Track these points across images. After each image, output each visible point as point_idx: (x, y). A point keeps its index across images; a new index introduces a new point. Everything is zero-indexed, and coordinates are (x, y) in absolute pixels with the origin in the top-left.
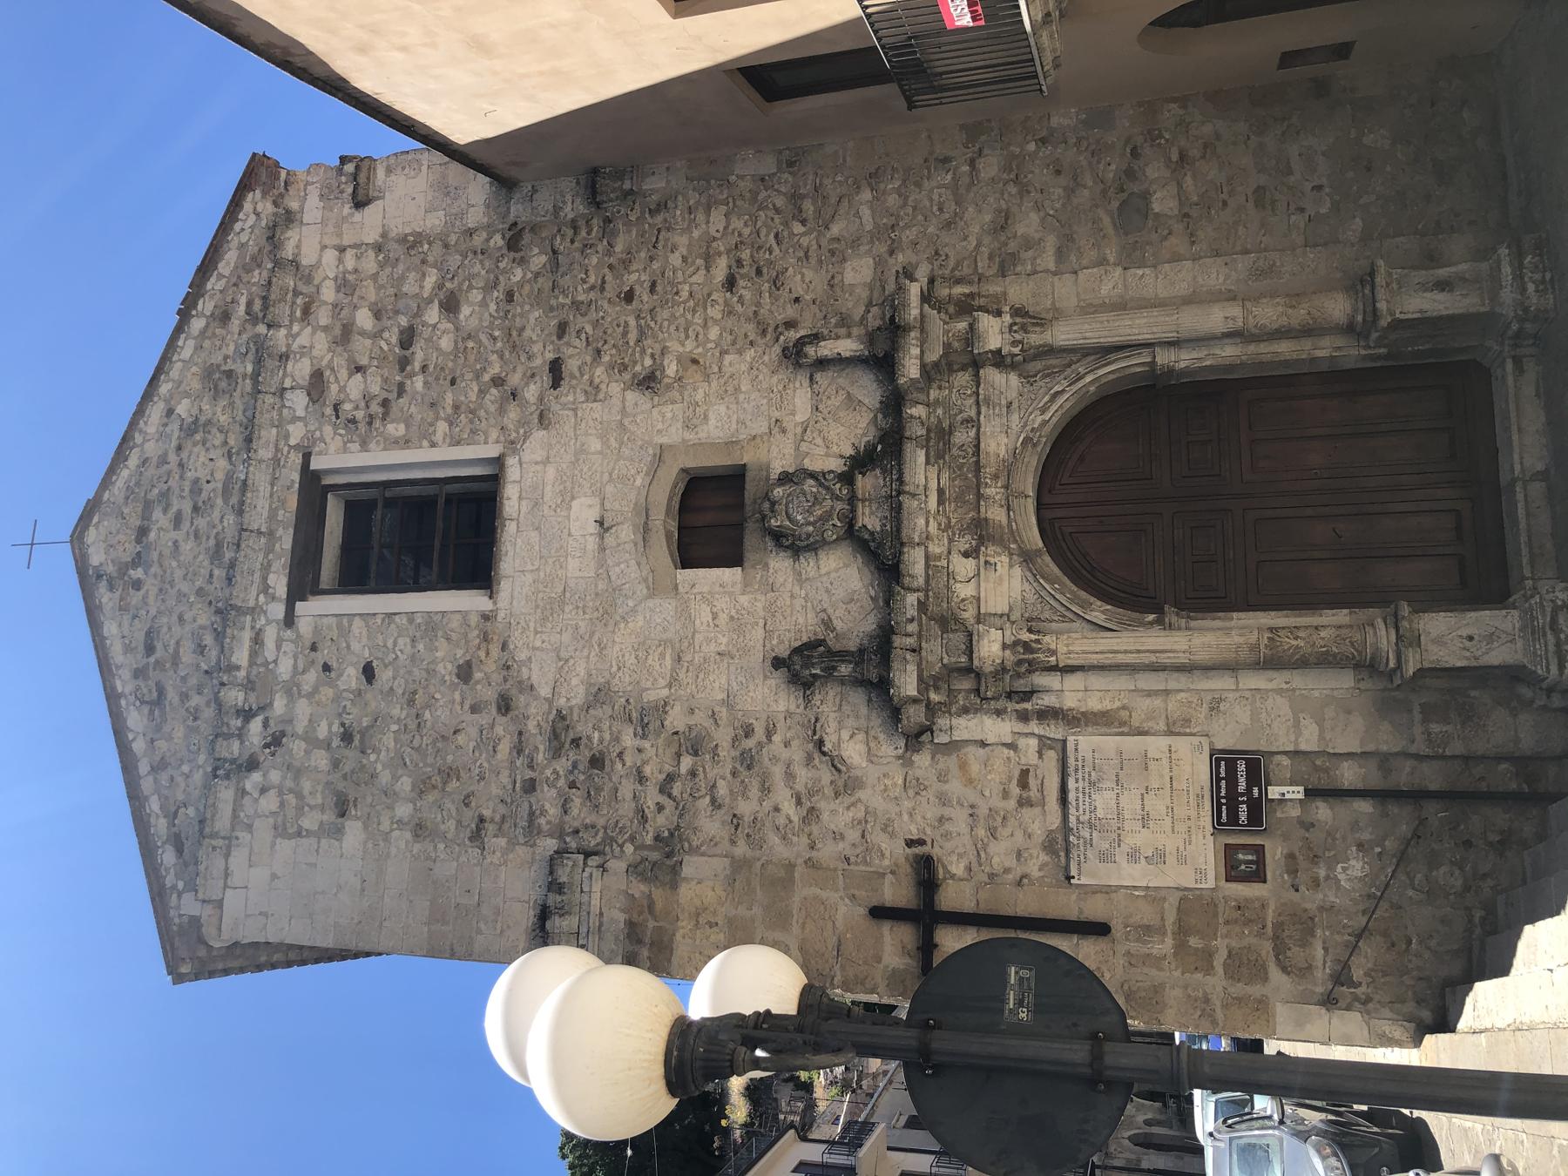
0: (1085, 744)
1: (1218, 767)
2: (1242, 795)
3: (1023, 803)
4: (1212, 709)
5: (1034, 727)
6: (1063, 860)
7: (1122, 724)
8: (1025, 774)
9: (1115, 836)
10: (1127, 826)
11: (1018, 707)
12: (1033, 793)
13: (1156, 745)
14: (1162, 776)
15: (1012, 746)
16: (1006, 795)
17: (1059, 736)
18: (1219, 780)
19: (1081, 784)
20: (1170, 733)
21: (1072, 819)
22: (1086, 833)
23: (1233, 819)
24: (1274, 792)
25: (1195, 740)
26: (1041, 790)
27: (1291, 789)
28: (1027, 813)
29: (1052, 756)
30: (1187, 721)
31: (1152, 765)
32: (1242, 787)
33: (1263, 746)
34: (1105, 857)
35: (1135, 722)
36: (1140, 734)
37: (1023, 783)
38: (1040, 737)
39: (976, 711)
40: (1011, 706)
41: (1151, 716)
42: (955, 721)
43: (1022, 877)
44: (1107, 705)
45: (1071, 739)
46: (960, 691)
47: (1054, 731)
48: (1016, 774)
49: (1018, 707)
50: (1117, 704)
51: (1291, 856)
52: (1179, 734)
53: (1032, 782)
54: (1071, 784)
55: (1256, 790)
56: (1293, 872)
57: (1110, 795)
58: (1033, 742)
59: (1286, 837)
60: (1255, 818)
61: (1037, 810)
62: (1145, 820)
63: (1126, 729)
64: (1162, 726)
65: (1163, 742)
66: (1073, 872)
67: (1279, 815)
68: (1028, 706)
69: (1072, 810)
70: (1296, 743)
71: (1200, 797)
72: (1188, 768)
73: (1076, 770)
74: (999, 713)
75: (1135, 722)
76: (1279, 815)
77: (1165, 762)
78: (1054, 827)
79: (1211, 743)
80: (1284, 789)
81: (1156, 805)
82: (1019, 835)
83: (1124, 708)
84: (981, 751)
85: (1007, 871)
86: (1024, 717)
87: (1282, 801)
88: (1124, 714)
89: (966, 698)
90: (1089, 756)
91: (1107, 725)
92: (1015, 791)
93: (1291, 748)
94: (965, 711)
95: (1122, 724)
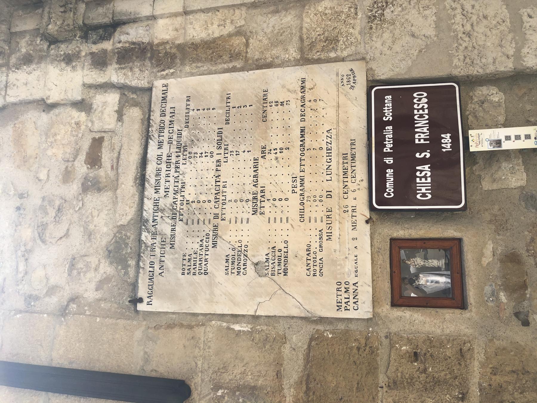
0: (178, 87)
1: (380, 104)
2: (422, 148)
3: (91, 186)
4: (371, 19)
5: (113, 74)
6: (132, 272)
7: (234, 56)
8: (97, 143)
9: (208, 229)
10: (230, 211)
11: (95, 48)
12: (105, 172)
13: (282, 81)
14: (287, 129)
15: (83, 105)
16: (67, 176)
17: (144, 83)
18: (381, 125)
19: (165, 150)
20: (304, 60)
21: (148, 205)
22: (165, 228)
23: (406, 189)
24: (481, 140)
25: (343, 68)
26: (116, 167)
27: (512, 131)
28: (94, 201)
29: (134, 114)
30: (332, 41)
31: (274, 113)
32: (422, 134)
33: (459, 68)
34: (193, 265)
35: (254, 53)
36: (260, 67)
37: (94, 160)
38: (122, 88)
39: (41, 59)
40: (86, 48)
41: (277, 40)
42: (12, 76)
43: (72, 300)
44: (215, 31)
45: (159, 84)
46: (22, 34)
47: (136, 77)
48: (86, 145)
49: (95, 48)
50: (229, 29)
51: (511, 259)
52: (319, 61)
53: (106, 157)
54: (153, 151)
55: (446, 139)
56: (518, 289)
57: (209, 163)
58: (112, 99)
59: (500, 225)
60: (445, 190)
61: (106, 197)
62: (257, 201)
63: (238, 64)
64: (293, 53)
65: (292, 75)
66: (142, 292)
67: (486, 185)
68: (107, 45)
69: (150, 191)
70: (518, 56)
71: (349, 158)
72: (331, 113)
73: (161, 129)
74: (69, 59)
75: (254, 53)
76: (486, 185)
77: (295, 107)
78: (124, 221)
79: (369, 71)
80: (500, 133)
81: (277, 176)
82: (77, 234)
83: (239, 32)
84: (44, 118)
85: (52, 290)
86: (100, 61)
87: (495, 156)
88: (238, 42)
89: (31, 43)
90: (181, 107)
91: (211, 60)
92: (81, 168)
93: (507, 66)
94: (27, 60)
95: (234, 56)
